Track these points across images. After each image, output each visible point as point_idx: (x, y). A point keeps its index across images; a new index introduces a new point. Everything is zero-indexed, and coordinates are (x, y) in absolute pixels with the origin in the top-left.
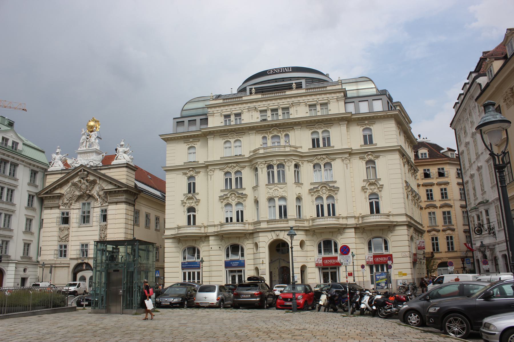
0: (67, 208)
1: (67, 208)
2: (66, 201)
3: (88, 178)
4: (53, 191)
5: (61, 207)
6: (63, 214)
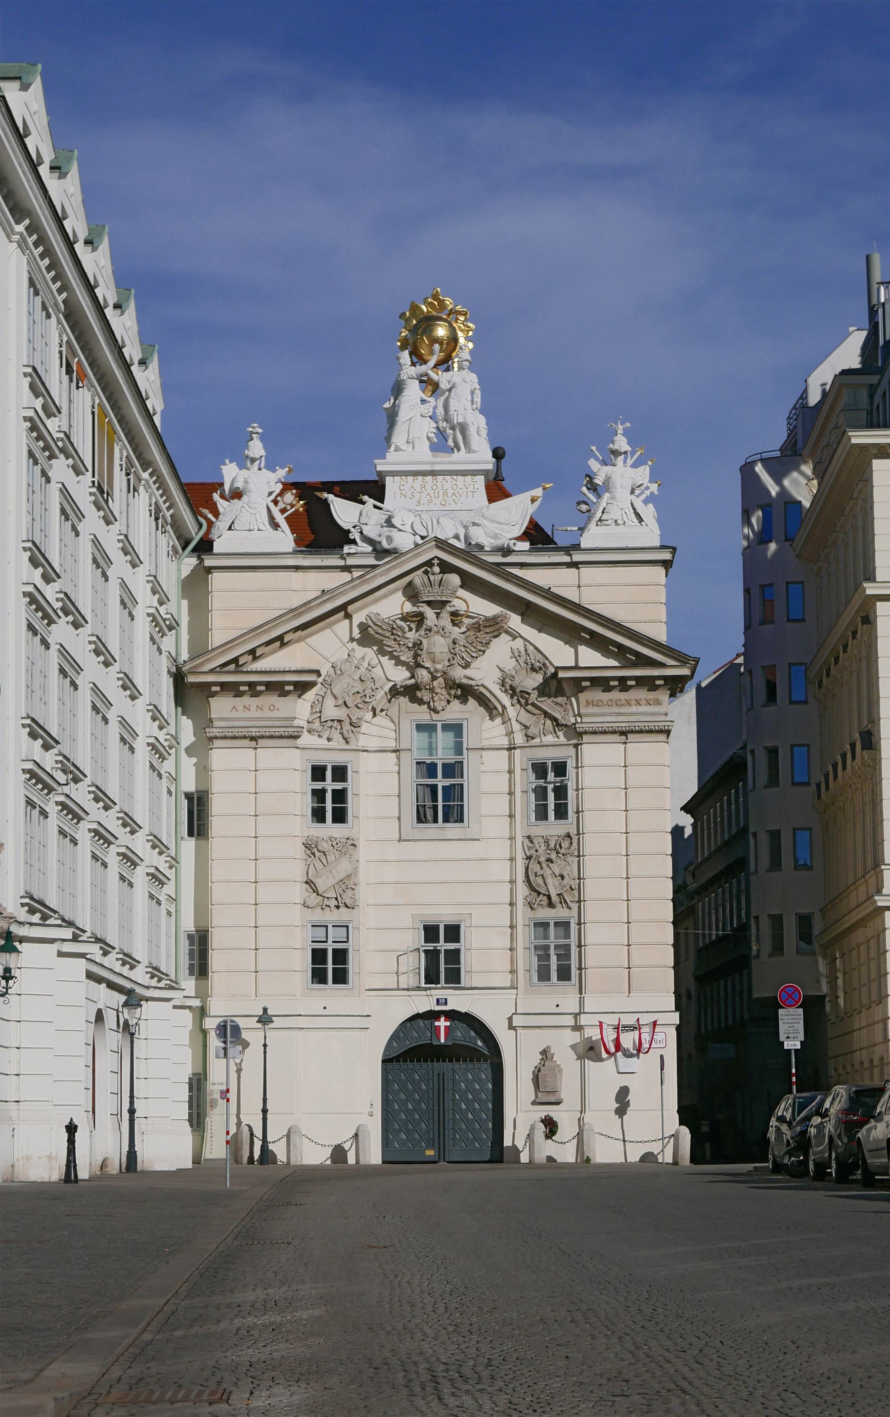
0: (332, 744)
1: (332, 744)
2: (331, 710)
5: (306, 739)
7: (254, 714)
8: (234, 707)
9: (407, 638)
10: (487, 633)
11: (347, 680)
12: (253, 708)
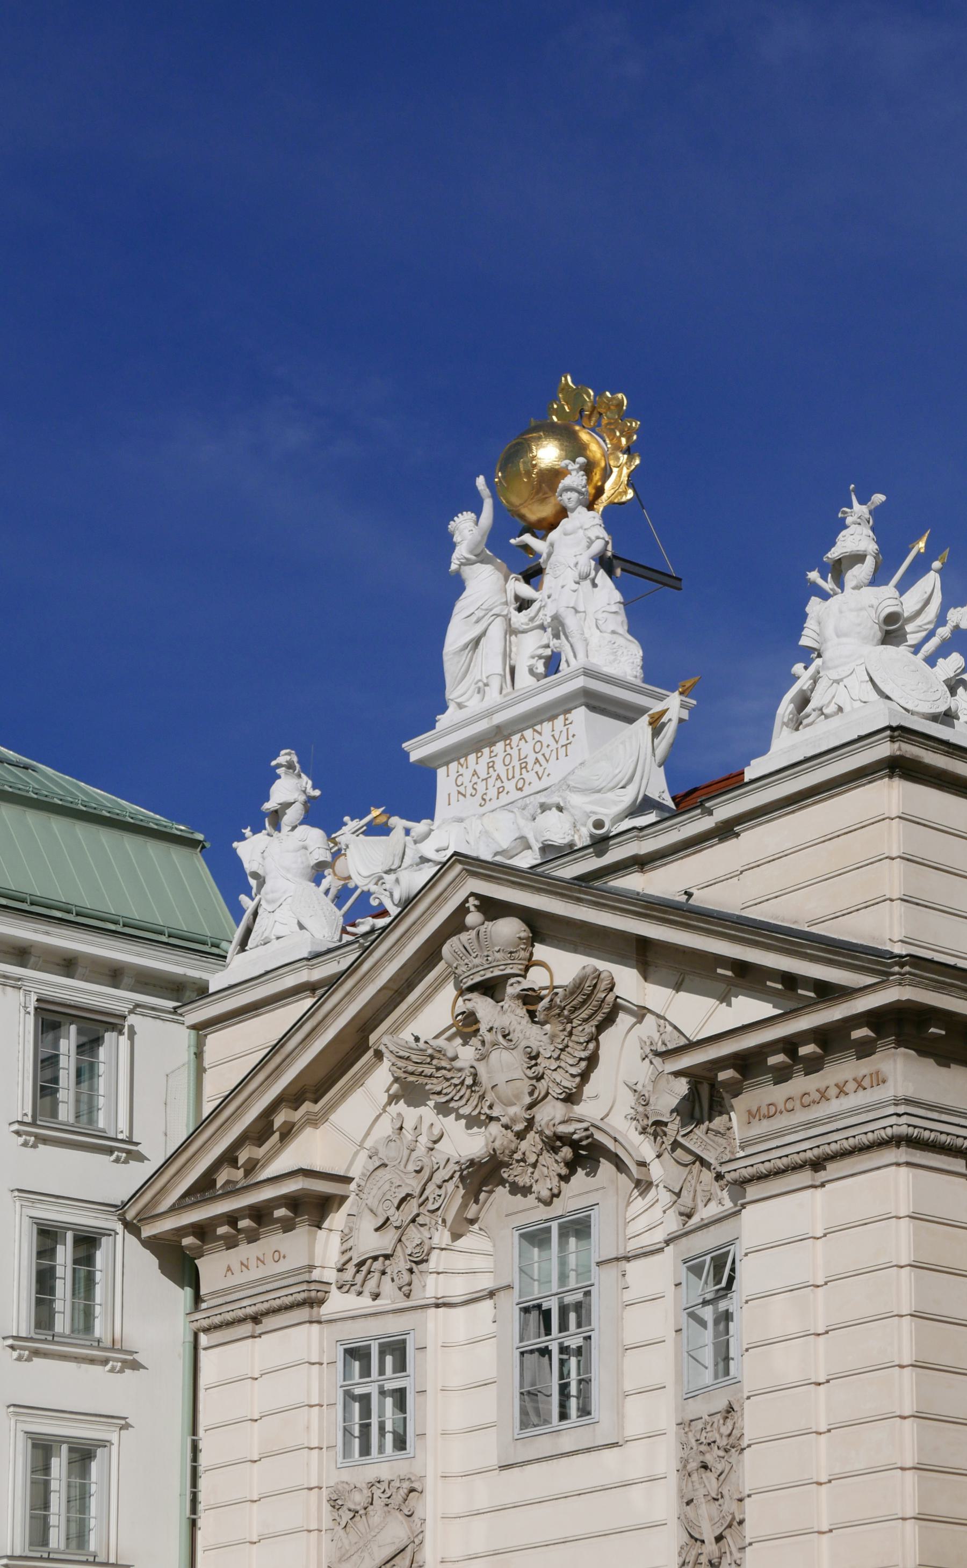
0: (383, 1303)
1: (383, 1303)
2: (370, 1242)
3: (537, 978)
5: (337, 1303)
7: (255, 1273)
8: (229, 1269)
9: (460, 1070)
10: (586, 1020)
11: (388, 1177)
12: (253, 1263)
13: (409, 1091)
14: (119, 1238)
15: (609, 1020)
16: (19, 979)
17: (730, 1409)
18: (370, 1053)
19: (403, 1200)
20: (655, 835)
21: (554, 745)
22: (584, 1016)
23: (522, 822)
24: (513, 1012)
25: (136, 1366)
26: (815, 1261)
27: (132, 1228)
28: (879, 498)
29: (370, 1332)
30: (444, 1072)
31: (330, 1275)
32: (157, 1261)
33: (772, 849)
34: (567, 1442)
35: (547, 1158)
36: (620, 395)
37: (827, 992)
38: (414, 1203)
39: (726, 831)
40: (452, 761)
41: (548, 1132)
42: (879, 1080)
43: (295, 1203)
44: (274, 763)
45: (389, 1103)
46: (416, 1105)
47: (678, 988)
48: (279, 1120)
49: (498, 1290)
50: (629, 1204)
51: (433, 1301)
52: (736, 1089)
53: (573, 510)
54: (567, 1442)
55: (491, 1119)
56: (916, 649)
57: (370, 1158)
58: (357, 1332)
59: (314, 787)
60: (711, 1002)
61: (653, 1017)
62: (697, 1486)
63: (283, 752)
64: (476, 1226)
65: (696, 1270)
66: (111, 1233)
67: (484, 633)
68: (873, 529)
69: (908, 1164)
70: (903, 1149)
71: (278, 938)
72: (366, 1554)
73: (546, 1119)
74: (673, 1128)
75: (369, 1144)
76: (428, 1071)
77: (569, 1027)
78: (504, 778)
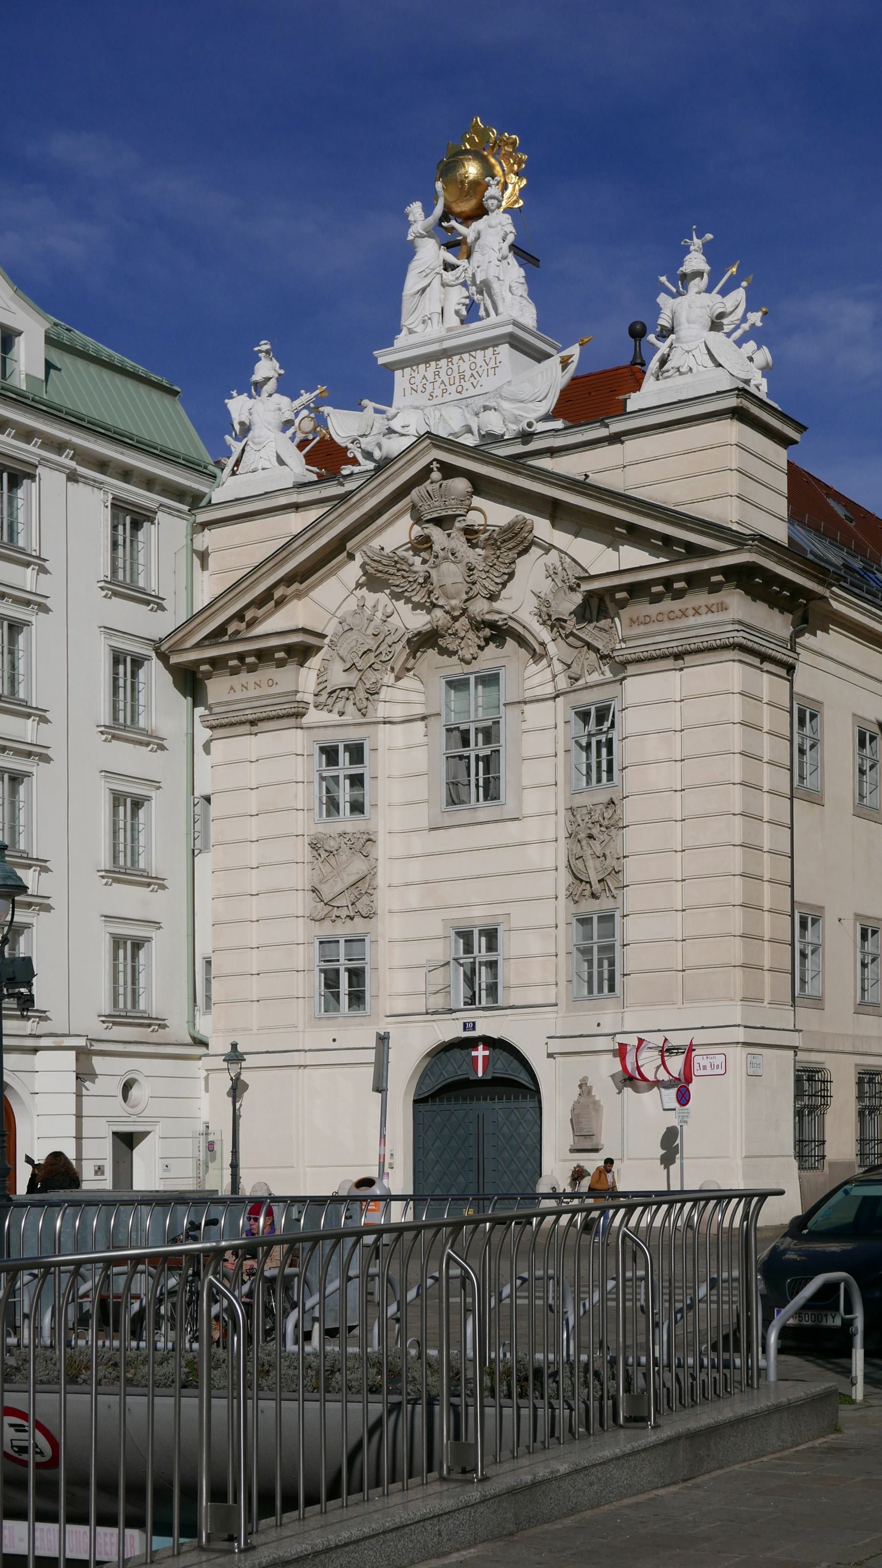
0: (346, 719)
1: (346, 719)
2: (338, 677)
3: (474, 518)
4: (251, 624)
5: (313, 716)
6: (330, 754)
7: (252, 693)
8: (232, 688)
9: (415, 572)
10: (510, 549)
11: (355, 637)
12: (251, 686)
13: (373, 581)
14: (153, 661)
15: (526, 551)
16: (102, 483)
17: (612, 802)
18: (345, 554)
19: (365, 653)
20: (565, 435)
21: (485, 367)
22: (510, 546)
23: (468, 416)
24: (458, 539)
25: (162, 748)
26: (673, 717)
27: (163, 657)
28: (709, 236)
29: (340, 737)
30: (403, 573)
31: (310, 698)
32: (171, 678)
33: (648, 454)
34: (482, 815)
35: (471, 635)
36: (514, 136)
37: (693, 551)
38: (372, 655)
39: (616, 439)
40: (407, 367)
41: (478, 619)
42: (723, 607)
43: (289, 649)
44: (256, 349)
45: (356, 589)
46: (375, 591)
47: (576, 535)
48: (278, 594)
49: (430, 716)
50: (526, 667)
51: (382, 719)
52: (622, 604)
53: (493, 211)
54: (482, 815)
55: (435, 606)
56: (728, 335)
57: (341, 623)
58: (331, 737)
59: (280, 368)
60: (601, 547)
61: (556, 552)
62: (585, 848)
63: (263, 342)
64: (412, 673)
65: (584, 716)
66: (149, 658)
67: (429, 285)
68: (703, 254)
69: (740, 661)
70: (736, 651)
71: (263, 469)
72: (339, 879)
73: (478, 610)
74: (571, 625)
75: (339, 614)
76: (392, 571)
77: (498, 552)
78: (447, 384)
